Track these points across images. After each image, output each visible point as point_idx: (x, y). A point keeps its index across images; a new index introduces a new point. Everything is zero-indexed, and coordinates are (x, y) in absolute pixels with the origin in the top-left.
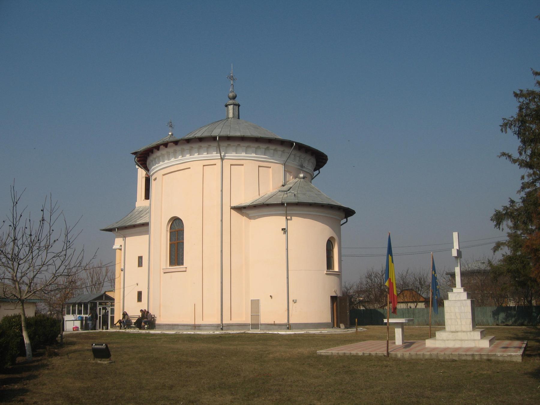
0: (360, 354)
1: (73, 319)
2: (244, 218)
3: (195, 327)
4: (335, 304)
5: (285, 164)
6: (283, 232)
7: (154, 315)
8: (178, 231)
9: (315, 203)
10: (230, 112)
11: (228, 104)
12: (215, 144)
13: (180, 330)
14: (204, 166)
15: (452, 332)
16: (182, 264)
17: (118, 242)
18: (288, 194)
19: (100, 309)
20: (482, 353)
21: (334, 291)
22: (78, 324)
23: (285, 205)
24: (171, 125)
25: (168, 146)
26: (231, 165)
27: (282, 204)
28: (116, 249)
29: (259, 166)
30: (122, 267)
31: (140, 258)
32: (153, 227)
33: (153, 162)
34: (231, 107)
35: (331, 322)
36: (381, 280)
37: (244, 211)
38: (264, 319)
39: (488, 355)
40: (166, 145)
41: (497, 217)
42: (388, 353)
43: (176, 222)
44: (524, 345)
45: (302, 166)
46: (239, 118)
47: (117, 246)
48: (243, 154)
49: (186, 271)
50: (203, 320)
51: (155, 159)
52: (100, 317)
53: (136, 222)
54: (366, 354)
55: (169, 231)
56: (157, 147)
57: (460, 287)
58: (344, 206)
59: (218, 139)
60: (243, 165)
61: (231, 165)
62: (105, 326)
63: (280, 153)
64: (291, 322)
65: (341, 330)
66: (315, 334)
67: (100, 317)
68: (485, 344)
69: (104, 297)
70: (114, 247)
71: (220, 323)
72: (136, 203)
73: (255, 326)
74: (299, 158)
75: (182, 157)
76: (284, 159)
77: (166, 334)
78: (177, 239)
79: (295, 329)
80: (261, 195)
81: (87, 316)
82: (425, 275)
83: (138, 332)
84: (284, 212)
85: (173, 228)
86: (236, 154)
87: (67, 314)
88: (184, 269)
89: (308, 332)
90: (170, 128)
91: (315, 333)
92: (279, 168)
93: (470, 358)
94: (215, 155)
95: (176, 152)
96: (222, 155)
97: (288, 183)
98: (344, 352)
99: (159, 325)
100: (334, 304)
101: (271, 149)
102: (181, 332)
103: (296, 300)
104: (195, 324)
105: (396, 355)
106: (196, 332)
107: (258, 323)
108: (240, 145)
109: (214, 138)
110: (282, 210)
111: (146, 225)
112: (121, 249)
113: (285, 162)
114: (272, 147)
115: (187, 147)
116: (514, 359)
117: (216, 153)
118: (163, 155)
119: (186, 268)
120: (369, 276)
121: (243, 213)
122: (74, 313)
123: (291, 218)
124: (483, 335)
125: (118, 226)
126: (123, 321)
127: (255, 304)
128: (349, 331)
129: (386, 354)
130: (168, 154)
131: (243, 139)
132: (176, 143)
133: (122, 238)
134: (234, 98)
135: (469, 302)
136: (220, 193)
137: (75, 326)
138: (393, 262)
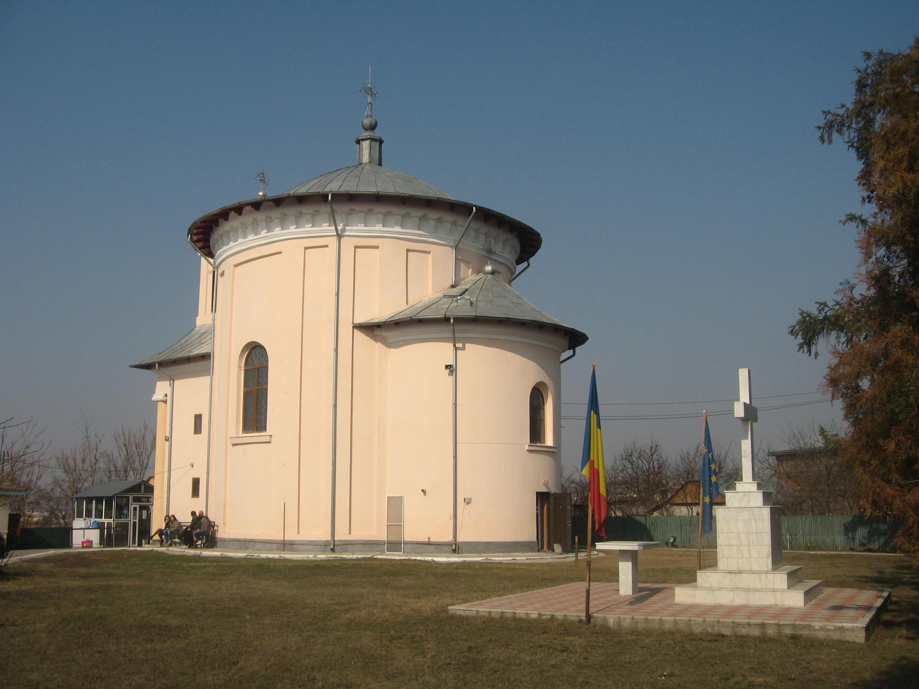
0: (534, 615)
1: (83, 526)
2: (379, 346)
3: (285, 545)
4: (546, 506)
5: (456, 246)
6: (448, 371)
7: (214, 523)
8: (258, 369)
9: (508, 318)
10: (364, 152)
11: (360, 138)
12: (325, 209)
13: (258, 550)
14: (306, 248)
15: (730, 572)
16: (265, 429)
17: (162, 389)
18: (459, 301)
19: (135, 509)
20: (782, 622)
21: (544, 483)
22: (94, 536)
23: (452, 321)
24: (263, 179)
25: (243, 212)
26: (356, 247)
27: (446, 320)
28: (158, 401)
29: (408, 251)
30: (168, 434)
31: (198, 418)
32: (218, 361)
33: (219, 242)
34: (366, 145)
35: (536, 540)
36: (649, 463)
37: (378, 332)
38: (413, 532)
39: (794, 626)
40: (239, 210)
41: (804, 325)
42: (589, 617)
43: (255, 352)
44: (879, 602)
45: (490, 251)
46: (380, 164)
47: (158, 395)
48: (379, 227)
49: (270, 442)
50: (298, 533)
51: (222, 236)
52: (136, 522)
53: (192, 352)
54: (546, 617)
55: (243, 368)
56: (224, 215)
57: (751, 480)
58: (565, 325)
59: (330, 198)
60: (377, 247)
61: (356, 247)
62: (145, 539)
63: (448, 226)
64: (461, 538)
65: (555, 557)
66: (501, 563)
67: (135, 523)
68: (795, 599)
69: (143, 487)
70: (155, 398)
71: (329, 538)
72: (197, 318)
73: (394, 545)
74: (486, 237)
75: (268, 232)
76: (457, 237)
77: (230, 558)
78: (256, 385)
79: (469, 552)
80: (411, 304)
81: (111, 521)
82: (723, 456)
83: (183, 554)
84: (450, 335)
85: (251, 363)
86: (365, 226)
87: (77, 517)
88: (267, 439)
89: (490, 559)
90: (261, 184)
91: (502, 562)
92: (449, 254)
93: (756, 632)
94: (326, 228)
95: (258, 224)
96: (339, 228)
97: (462, 282)
98: (501, 610)
99: (223, 540)
100: (544, 507)
101: (431, 219)
102: (256, 555)
103: (470, 499)
105: (605, 620)
106: (282, 556)
107: (400, 540)
108: (372, 210)
109: (323, 198)
110: (446, 330)
111: (206, 357)
112: (166, 402)
113: (457, 242)
114: (433, 215)
115: (276, 213)
116: (850, 637)
117: (328, 224)
118: (235, 230)
119: (271, 436)
120: (628, 457)
122: (89, 515)
123: (464, 346)
124: (794, 579)
125: (159, 360)
126: (167, 533)
127: (395, 505)
128: (569, 557)
129: (584, 618)
130: (244, 226)
131: (378, 199)
132: (257, 206)
133: (168, 382)
134: (373, 127)
135: (766, 512)
136: (334, 298)
137: (85, 540)
138: (599, 426)
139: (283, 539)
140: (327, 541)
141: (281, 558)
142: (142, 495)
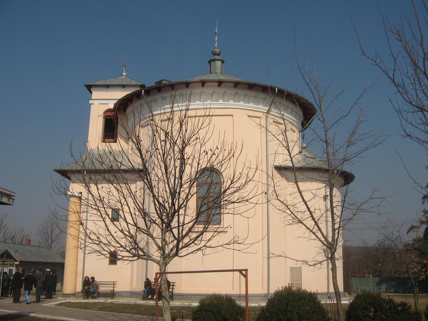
11: (216, 58)
12: (262, 95)
25: (205, 85)
34: (219, 63)
37: (284, 172)
56: (187, 85)
104: (241, 293)
106: (260, 304)
121: (282, 174)
139: (239, 293)
140: (265, 294)
141: (259, 306)
142: (5, 260)
